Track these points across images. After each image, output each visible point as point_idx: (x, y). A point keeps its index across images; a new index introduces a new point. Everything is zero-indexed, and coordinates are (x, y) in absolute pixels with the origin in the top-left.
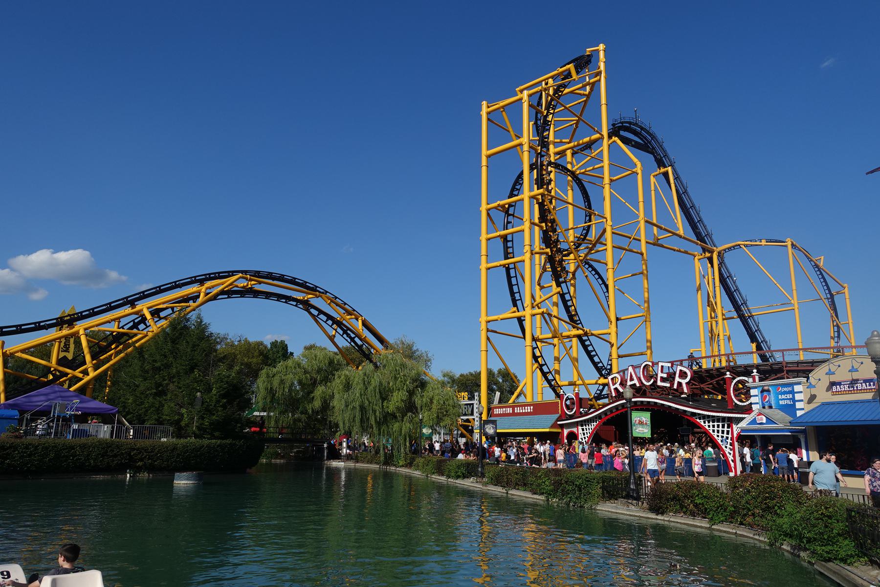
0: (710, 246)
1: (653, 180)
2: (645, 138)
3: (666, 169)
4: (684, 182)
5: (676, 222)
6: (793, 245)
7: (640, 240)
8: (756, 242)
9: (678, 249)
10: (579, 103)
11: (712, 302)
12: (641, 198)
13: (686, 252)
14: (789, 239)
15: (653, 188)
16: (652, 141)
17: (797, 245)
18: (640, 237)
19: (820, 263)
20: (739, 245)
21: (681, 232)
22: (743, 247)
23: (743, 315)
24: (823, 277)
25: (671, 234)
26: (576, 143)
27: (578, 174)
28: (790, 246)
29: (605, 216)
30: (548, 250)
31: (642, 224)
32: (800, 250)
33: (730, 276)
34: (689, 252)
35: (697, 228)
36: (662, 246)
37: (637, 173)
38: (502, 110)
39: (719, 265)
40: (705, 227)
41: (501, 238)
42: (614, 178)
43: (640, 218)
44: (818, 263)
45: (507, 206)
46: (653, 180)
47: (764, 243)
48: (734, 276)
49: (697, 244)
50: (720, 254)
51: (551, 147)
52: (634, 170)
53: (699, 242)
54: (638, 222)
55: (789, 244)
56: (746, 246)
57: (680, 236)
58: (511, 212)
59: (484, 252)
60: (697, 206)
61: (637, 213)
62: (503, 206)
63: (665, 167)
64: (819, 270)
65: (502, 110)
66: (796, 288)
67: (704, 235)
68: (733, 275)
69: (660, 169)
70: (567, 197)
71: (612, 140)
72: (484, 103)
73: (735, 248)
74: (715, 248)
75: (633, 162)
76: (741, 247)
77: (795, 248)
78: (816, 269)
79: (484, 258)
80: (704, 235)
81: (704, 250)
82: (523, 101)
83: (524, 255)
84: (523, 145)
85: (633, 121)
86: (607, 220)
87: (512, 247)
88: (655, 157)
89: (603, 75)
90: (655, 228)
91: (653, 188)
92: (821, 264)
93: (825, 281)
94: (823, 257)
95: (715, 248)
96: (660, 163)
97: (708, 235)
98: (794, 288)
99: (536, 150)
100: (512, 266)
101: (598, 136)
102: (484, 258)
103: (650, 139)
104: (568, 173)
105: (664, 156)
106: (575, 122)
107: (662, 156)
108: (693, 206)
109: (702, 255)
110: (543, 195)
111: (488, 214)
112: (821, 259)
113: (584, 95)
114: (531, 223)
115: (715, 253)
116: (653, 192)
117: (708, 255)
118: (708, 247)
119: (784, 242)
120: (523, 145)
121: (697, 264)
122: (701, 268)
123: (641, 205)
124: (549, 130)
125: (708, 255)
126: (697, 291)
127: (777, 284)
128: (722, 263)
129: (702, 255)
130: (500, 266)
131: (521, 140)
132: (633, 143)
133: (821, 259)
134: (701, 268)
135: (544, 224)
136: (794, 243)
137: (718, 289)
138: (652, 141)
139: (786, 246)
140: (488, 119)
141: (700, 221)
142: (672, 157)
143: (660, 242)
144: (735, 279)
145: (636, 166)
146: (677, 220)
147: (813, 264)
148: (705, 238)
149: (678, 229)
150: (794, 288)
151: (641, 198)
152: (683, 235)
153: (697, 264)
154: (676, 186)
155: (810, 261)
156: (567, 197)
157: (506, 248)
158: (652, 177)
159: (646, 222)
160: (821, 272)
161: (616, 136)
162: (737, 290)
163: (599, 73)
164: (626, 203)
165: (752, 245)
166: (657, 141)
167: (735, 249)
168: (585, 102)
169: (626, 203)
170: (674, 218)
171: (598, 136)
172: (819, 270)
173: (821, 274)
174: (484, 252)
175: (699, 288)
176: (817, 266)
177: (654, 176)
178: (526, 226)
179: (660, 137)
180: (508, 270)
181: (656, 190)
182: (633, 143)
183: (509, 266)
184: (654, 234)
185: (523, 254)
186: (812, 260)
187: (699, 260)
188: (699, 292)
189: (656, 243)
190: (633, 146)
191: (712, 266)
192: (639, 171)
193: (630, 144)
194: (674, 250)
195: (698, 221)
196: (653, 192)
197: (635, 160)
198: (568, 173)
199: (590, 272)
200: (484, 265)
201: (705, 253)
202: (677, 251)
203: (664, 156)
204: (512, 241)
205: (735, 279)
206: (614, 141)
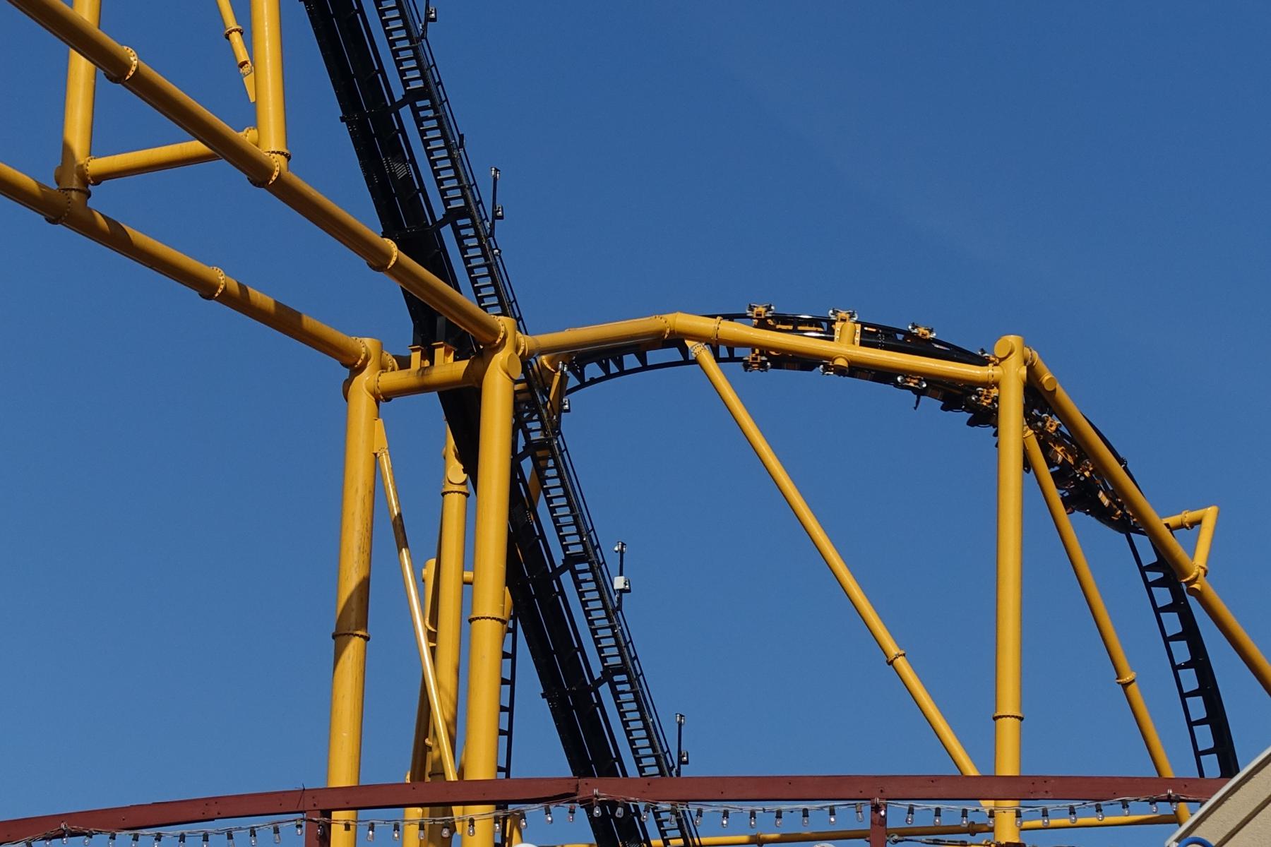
0: (466, 300)
5: (242, 55)
9: (233, 285)
11: (440, 762)
14: (1013, 340)
17: (1063, 395)
19: (1192, 556)
20: (677, 340)
22: (706, 356)
24: (1200, 662)
25: (196, 147)
34: (310, 322)
35: (394, 146)
36: (117, 240)
39: (515, 468)
40: (454, 145)
44: (1175, 544)
48: (613, 564)
49: (377, 260)
53: (391, 245)
56: (725, 351)
57: (256, 171)
64: (1179, 605)
67: (440, 213)
68: (609, 551)
73: (653, 357)
74: (504, 324)
76: (688, 360)
78: (1164, 596)
80: (440, 213)
90: (81, 68)
92: (1197, 559)
93: (1209, 690)
94: (1210, 515)
95: (504, 324)
97: (463, 212)
98: (1009, 702)
109: (404, 363)
112: (1199, 522)
115: (500, 359)
117: (448, 367)
119: (983, 362)
125: (448, 367)
126: (341, 637)
127: (901, 663)
129: (404, 363)
133: (1199, 522)
136: (1046, 376)
137: (488, 638)
143: (102, 204)
144: (619, 583)
147: (1149, 557)
148: (447, 232)
149: (251, 116)
150: (1009, 702)
152: (279, 163)
167: (645, 367)
170: (231, 23)
172: (1179, 605)
173: (1190, 633)
184: (67, 150)
187: (383, 397)
188: (354, 647)
191: (470, 456)
194: (206, 289)
201: (429, 355)
205: (619, 583)
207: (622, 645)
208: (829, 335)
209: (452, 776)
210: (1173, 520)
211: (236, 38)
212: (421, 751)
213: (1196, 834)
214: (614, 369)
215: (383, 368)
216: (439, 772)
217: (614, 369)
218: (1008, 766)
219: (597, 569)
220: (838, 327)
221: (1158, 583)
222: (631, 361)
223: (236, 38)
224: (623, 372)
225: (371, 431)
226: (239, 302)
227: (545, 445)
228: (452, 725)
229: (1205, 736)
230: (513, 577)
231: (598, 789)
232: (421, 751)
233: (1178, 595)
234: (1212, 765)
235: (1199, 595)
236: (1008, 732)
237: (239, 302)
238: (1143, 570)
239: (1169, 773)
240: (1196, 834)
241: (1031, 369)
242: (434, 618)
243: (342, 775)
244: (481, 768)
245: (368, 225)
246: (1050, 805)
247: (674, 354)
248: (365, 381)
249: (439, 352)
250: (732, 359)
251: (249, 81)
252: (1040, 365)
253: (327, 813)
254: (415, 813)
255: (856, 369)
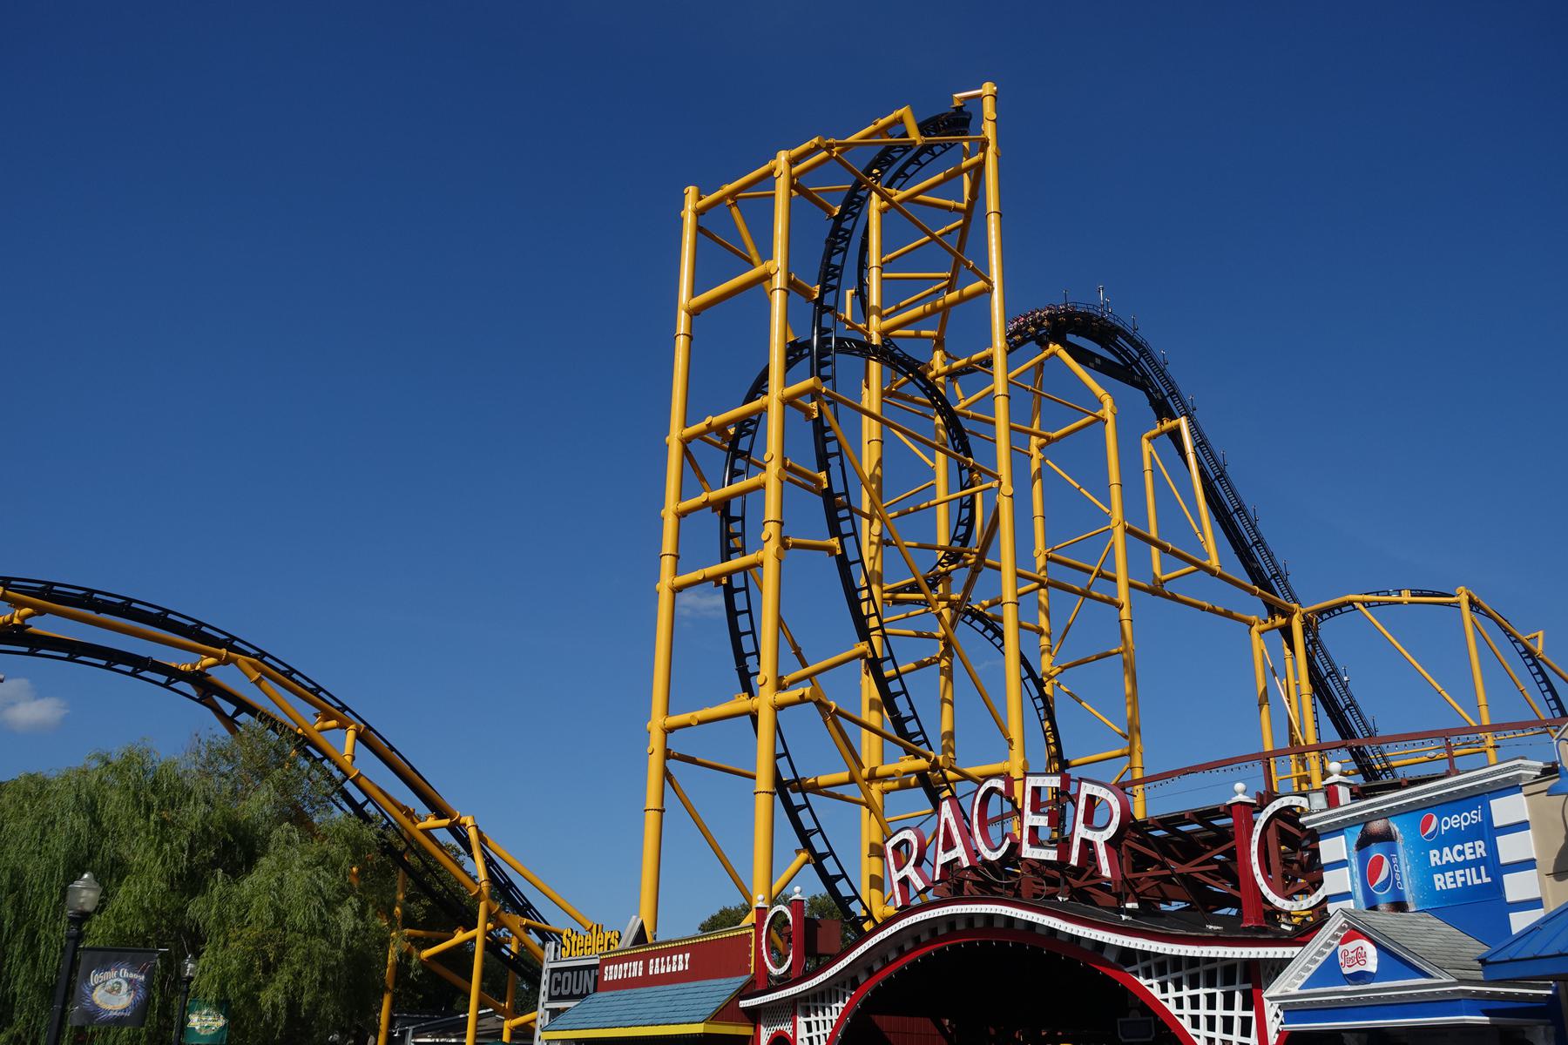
0: (1282, 600)
1: (1147, 447)
2: (1125, 352)
3: (1174, 422)
4: (1219, 453)
5: (1202, 540)
6: (1472, 602)
7: (1114, 580)
8: (1389, 595)
10: (949, 232)
11: (1298, 739)
12: (1114, 477)
13: (1227, 614)
15: (1147, 465)
16: (1142, 359)
18: (1116, 573)
19: (1537, 647)
20: (1351, 603)
21: (1214, 562)
22: (1361, 607)
23: (1370, 766)
24: (1546, 680)
25: (1193, 568)
26: (928, 307)
27: (934, 378)
28: (1465, 606)
29: (999, 474)
30: (835, 542)
31: (1119, 537)
32: (1489, 615)
33: (1334, 672)
34: (1235, 613)
36: (1173, 598)
37: (1103, 420)
38: (730, 202)
40: (1270, 556)
41: (714, 510)
42: (1055, 435)
43: (1114, 523)
44: (1529, 644)
45: (732, 431)
46: (1147, 447)
47: (1406, 597)
49: (1253, 593)
50: (1308, 626)
51: (874, 319)
52: (1097, 414)
54: (1110, 532)
55: (1464, 599)
56: (1367, 604)
57: (1212, 572)
58: (744, 444)
59: (668, 545)
60: (1249, 507)
61: (1108, 511)
62: (721, 429)
63: (1176, 418)
64: (1535, 663)
65: (730, 202)
66: (1487, 701)
68: (1341, 669)
69: (1162, 423)
70: (935, 463)
71: (1047, 352)
72: (691, 191)
73: (1344, 609)
74: (1295, 606)
75: (1096, 397)
76: (1355, 609)
77: (1477, 612)
78: (1529, 661)
79: (667, 563)
81: (1273, 609)
82: (776, 175)
83: (762, 548)
84: (772, 275)
85: (1095, 313)
86: (1000, 483)
87: (742, 534)
88: (1149, 395)
89: (991, 149)
90: (1155, 550)
91: (1147, 465)
92: (1539, 648)
93: (1551, 689)
94: (1540, 634)
95: (1295, 606)
96: (1163, 410)
97: (1277, 574)
98: (1482, 700)
99: (807, 294)
100: (738, 581)
101: (980, 284)
102: (667, 563)
103: (1137, 354)
104: (911, 375)
105: (1170, 395)
106: (946, 282)
107: (1166, 394)
108: (1241, 509)
109: (1266, 622)
110: (814, 394)
111: (686, 452)
112: (1537, 636)
113: (956, 209)
114: (784, 466)
116: (1148, 475)
117: (1280, 621)
118: (1277, 602)
119: (1453, 596)
120: (772, 275)
121: (1258, 644)
122: (1265, 651)
123: (1115, 492)
124: (844, 250)
125: (1280, 621)
126: (1261, 705)
127: (1443, 692)
128: (1313, 643)
129: (1266, 622)
130: (705, 580)
131: (769, 264)
132: (1098, 361)
133: (1537, 636)
134: (1265, 651)
135: (823, 475)
136: (1475, 598)
137: (1307, 701)
138: (1142, 359)
139: (1457, 605)
140: (699, 229)
141: (1260, 541)
142: (1188, 398)
143: (1168, 588)
144: (1346, 679)
145: (1100, 404)
146: (1203, 534)
147: (1522, 649)
148: (1273, 581)
149: (1208, 557)
150: (1482, 700)
151: (1114, 477)
152: (1218, 569)
153: (1258, 644)
154: (1199, 462)
155: (1513, 642)
156: (935, 463)
157: (727, 536)
158: (1145, 441)
159: (1128, 531)
160: (1539, 667)
161: (1056, 342)
162: (1352, 704)
163: (985, 144)
164: (1082, 490)
165: (1380, 603)
166: (1151, 359)
167: (1342, 613)
168: (963, 229)
169: (1082, 490)
171: (980, 284)
172: (1535, 663)
173: (1541, 672)
174: (668, 545)
175: (1264, 699)
176: (1529, 653)
177: (1149, 439)
178: (771, 476)
179: (1160, 352)
180: (729, 592)
181: (1155, 469)
182: (1098, 361)
183: (730, 579)
184: (1155, 574)
185: (760, 545)
186: (1518, 640)
187: (1261, 633)
188: (1265, 708)
189: (1157, 590)
190: (1097, 368)
191: (1291, 647)
192: (1109, 417)
193: (1091, 364)
194: (1202, 608)
195: (1255, 544)
196: (1148, 475)
197: (1099, 391)
198: (911, 375)
199: (991, 640)
200: (666, 580)
201: (1273, 618)
202: (1209, 610)
203: (1170, 395)
204: (742, 519)
205: (1346, 679)
206: (1054, 354)
207: (1350, 698)
208: (1400, 595)
209: (1303, 744)
210: (1528, 637)
211: (1199, 535)
212: (1291, 737)
213: (1563, 736)
214: (1332, 615)
215: (1260, 624)
216: (1298, 742)
217: (1332, 615)
218: (1486, 722)
219: (1338, 675)
220: (1402, 592)
221: (1527, 657)
222: (1337, 611)
223: (1199, 535)
224: (1335, 615)
225: (1259, 643)
226: (1213, 611)
227: (1315, 640)
228: (1300, 728)
229: (1553, 704)
230: (1312, 681)
231: (1353, 743)
232: (1291, 737)
233: (1534, 659)
234: (1557, 714)
235: (1542, 659)
236: (1484, 710)
237: (1213, 611)
238: (1520, 654)
239: (1543, 718)
240: (1563, 736)
241: (1470, 596)
242: (1288, 696)
243: (1268, 747)
244: (1312, 741)
245: (1248, 582)
246: (1506, 732)
247: (1351, 607)
248: (1255, 629)
249: (1277, 617)
250: (1369, 606)
251: (1205, 547)
252: (1473, 595)
253: (1268, 759)
254: (1292, 757)
255: (1410, 603)
